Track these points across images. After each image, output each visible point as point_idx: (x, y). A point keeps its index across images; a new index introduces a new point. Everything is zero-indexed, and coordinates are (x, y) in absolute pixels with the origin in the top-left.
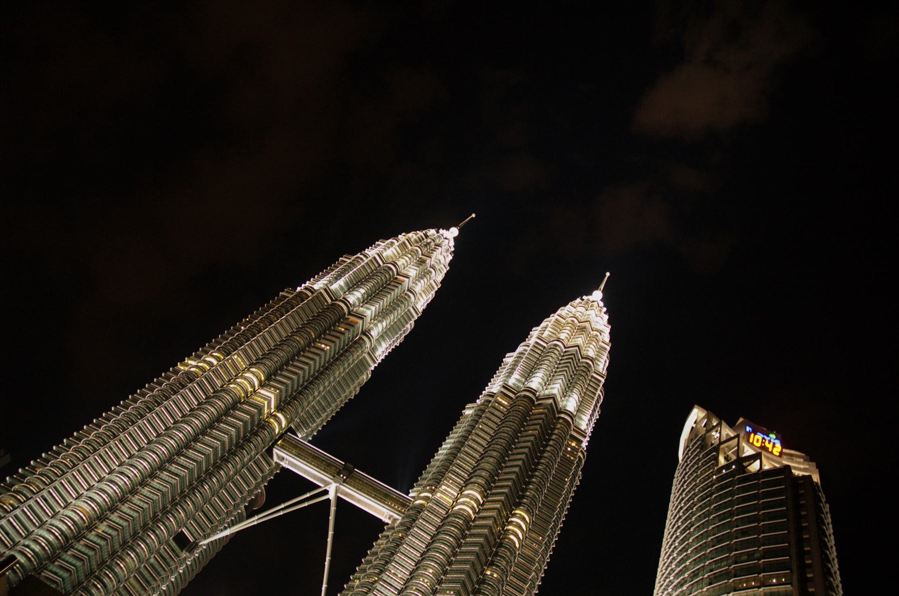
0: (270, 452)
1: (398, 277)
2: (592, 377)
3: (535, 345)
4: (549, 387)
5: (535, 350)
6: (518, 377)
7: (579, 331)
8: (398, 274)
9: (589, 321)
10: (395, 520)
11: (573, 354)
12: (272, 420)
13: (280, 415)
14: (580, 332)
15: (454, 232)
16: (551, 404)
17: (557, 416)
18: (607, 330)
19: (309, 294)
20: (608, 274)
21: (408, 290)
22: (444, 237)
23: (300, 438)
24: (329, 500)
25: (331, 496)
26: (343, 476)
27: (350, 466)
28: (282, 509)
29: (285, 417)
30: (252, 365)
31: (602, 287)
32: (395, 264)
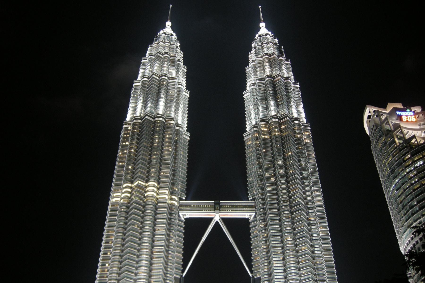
0: (179, 216)
1: (171, 81)
2: (293, 87)
8: (169, 80)
10: (250, 215)
12: (172, 202)
13: (173, 197)
15: (169, 24)
16: (288, 120)
17: (293, 124)
19: (139, 121)
20: (260, 7)
21: (179, 84)
22: (170, 34)
23: (185, 200)
26: (217, 208)
27: (218, 201)
29: (175, 196)
30: (147, 182)
31: (262, 18)
32: (165, 75)
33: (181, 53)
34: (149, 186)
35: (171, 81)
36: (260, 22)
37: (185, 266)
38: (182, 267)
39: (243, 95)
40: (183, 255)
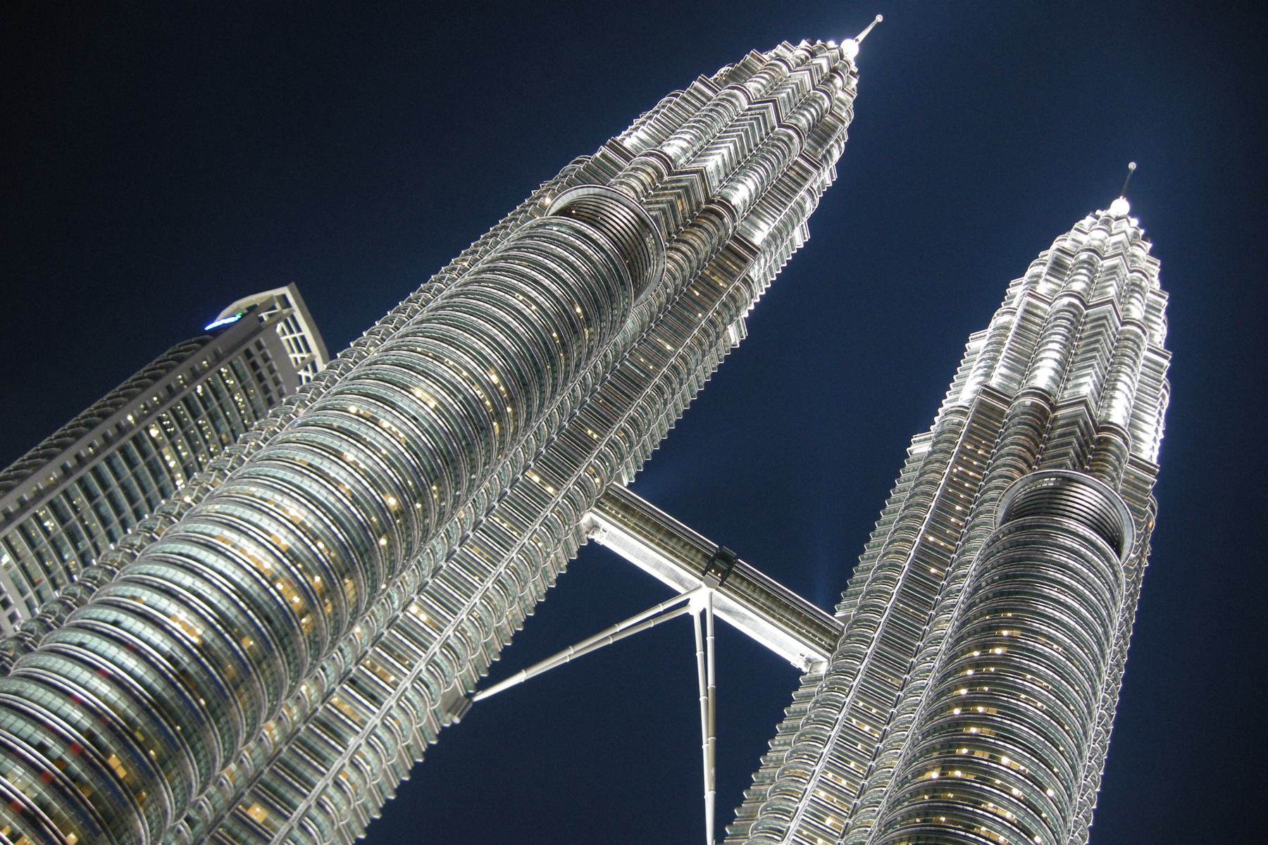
2: (1146, 358)
3: (1027, 308)
4: (1070, 385)
5: (1028, 317)
6: (1004, 371)
7: (1104, 274)
9: (1121, 254)
11: (1105, 318)
14: (1107, 275)
18: (1155, 270)
20: (1132, 166)
25: (694, 610)
28: (613, 635)
38: (490, 670)
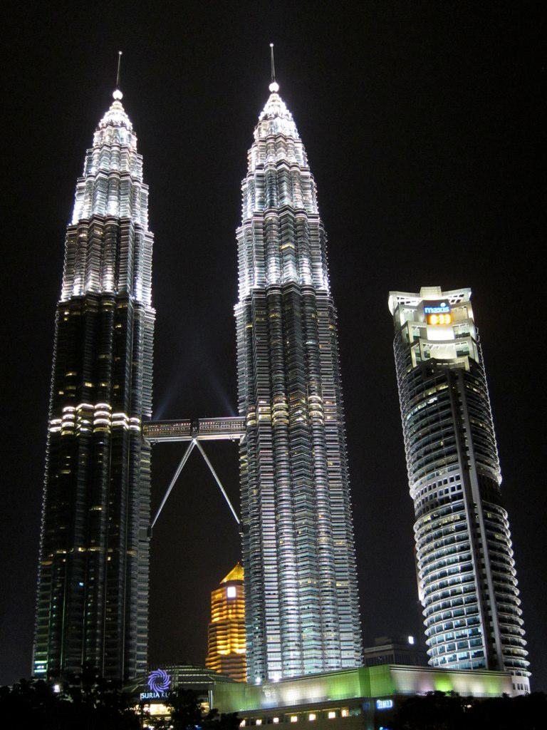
1: (123, 226)
20: (272, 45)
24: (196, 446)
31: (273, 73)
33: (140, 159)
34: (99, 409)
35: (123, 226)
36: (271, 82)
37: (153, 513)
39: (236, 235)
40: (151, 497)
